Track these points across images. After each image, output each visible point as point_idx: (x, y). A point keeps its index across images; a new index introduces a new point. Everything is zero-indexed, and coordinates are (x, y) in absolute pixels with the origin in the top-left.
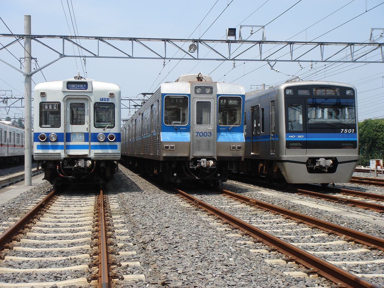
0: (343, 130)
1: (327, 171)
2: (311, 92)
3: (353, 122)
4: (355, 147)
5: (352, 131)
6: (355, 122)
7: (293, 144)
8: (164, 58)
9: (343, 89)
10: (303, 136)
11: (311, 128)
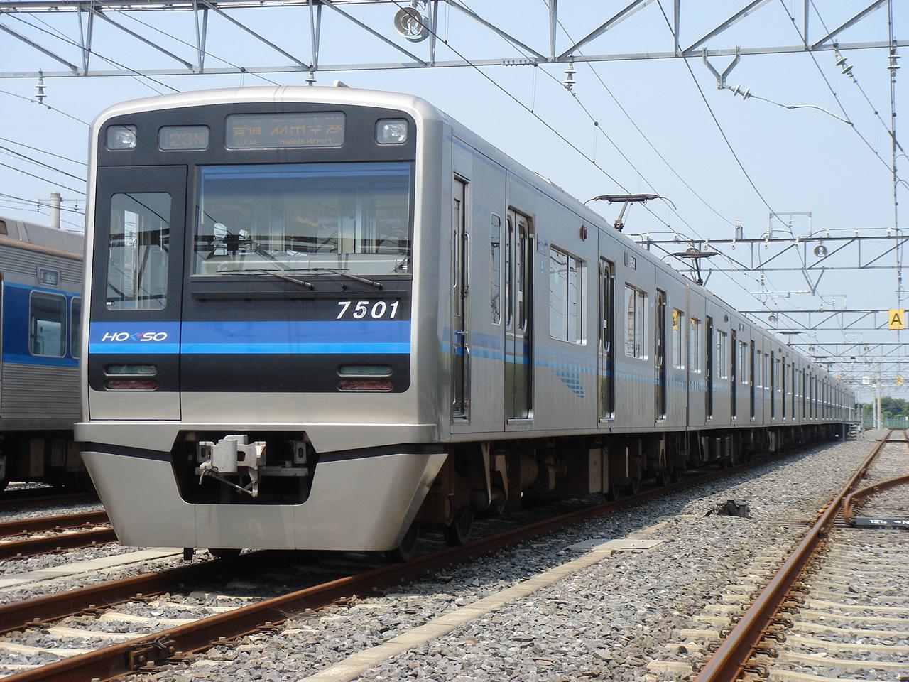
0: (347, 304)
1: (255, 492)
2: (218, 136)
3: (401, 267)
4: (399, 383)
5: (389, 309)
6: (405, 267)
7: (123, 373)
8: (312, 69)
9: (363, 122)
10: (166, 335)
11: (202, 299)
